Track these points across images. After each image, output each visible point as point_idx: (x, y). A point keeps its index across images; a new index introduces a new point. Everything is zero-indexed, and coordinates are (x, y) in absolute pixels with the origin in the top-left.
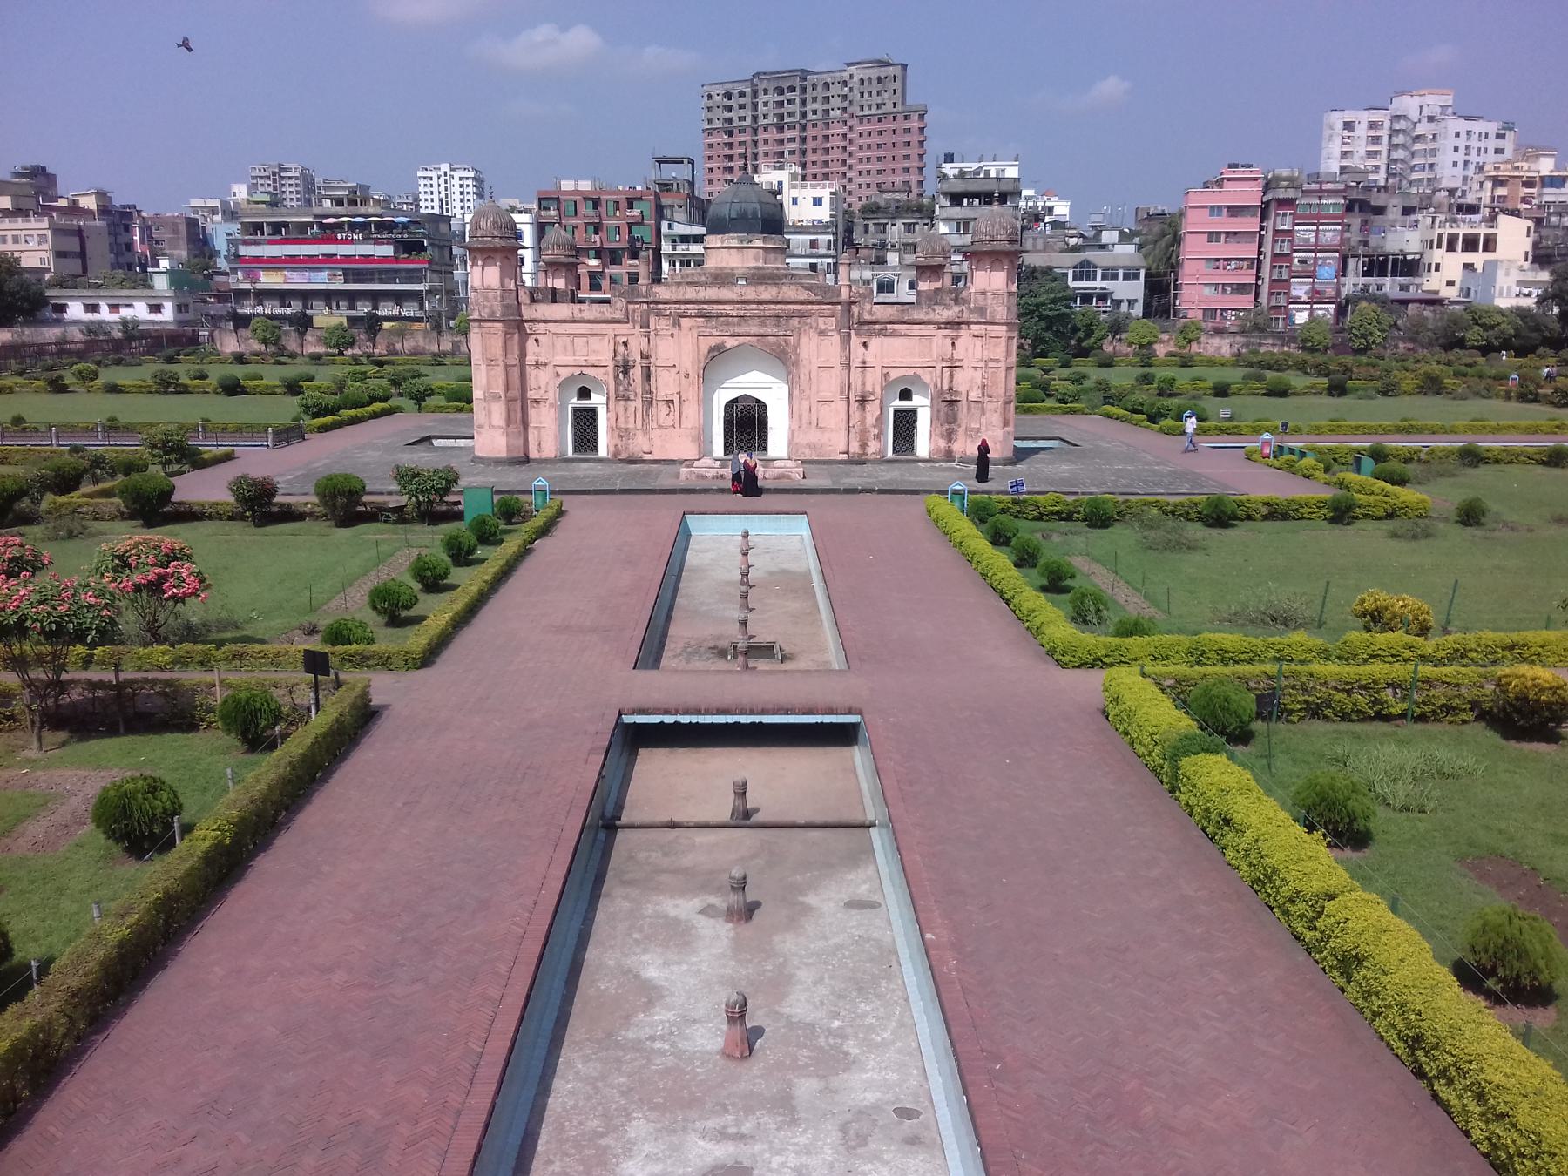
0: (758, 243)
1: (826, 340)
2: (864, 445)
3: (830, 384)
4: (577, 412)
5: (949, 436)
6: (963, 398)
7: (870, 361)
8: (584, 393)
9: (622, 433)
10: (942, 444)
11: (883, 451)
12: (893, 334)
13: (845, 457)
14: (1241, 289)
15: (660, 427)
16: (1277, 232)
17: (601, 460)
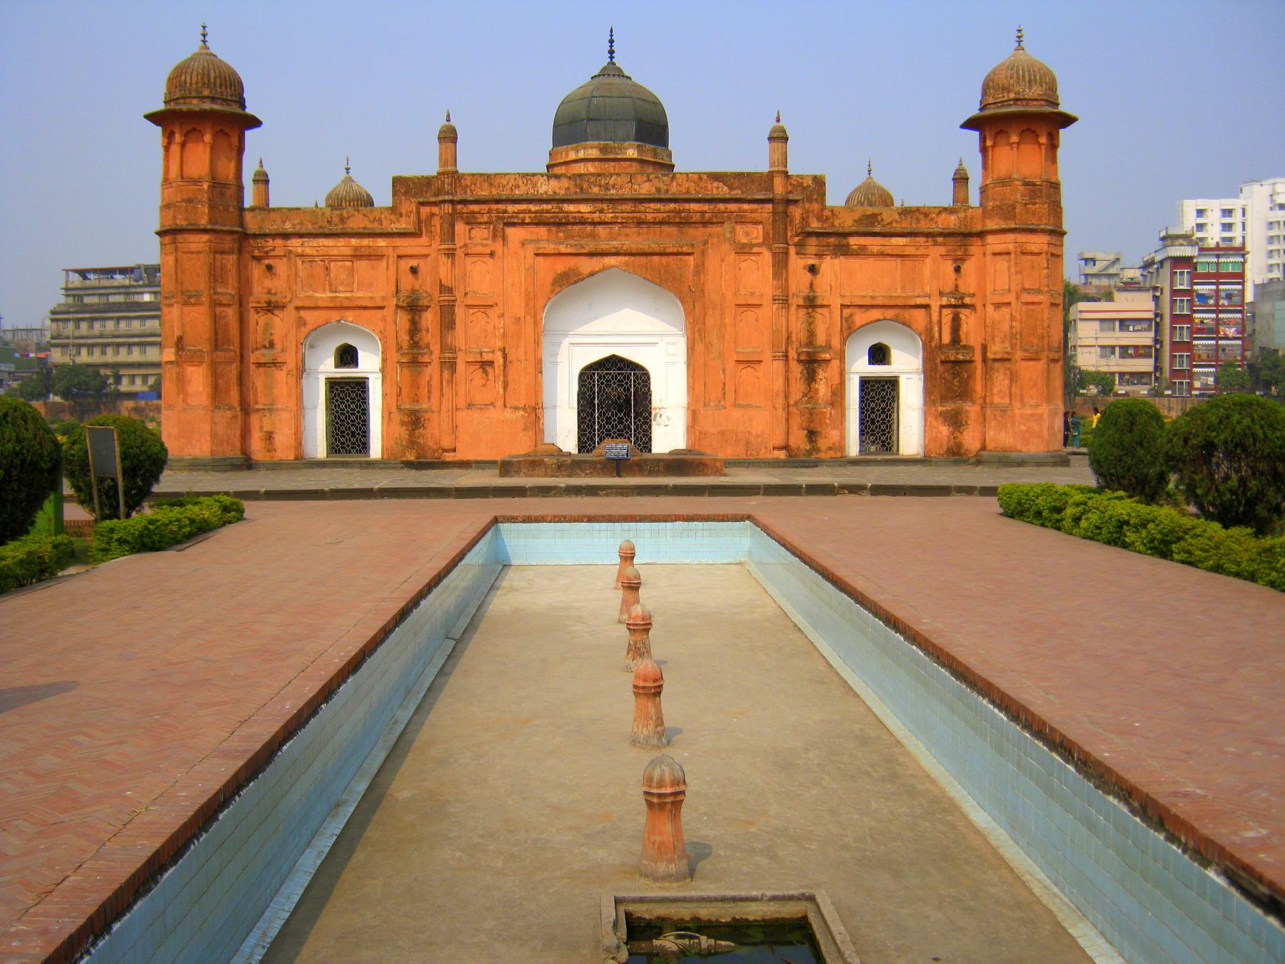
0: (632, 153)
1: (747, 264)
2: (812, 435)
3: (757, 332)
4: (334, 386)
5: (956, 421)
6: (978, 357)
7: (823, 295)
8: (347, 356)
9: (412, 421)
10: (945, 430)
11: (841, 447)
12: (862, 252)
13: (782, 455)
14: (1139, 352)
15: (470, 406)
16: (1175, 292)
17: (372, 464)
